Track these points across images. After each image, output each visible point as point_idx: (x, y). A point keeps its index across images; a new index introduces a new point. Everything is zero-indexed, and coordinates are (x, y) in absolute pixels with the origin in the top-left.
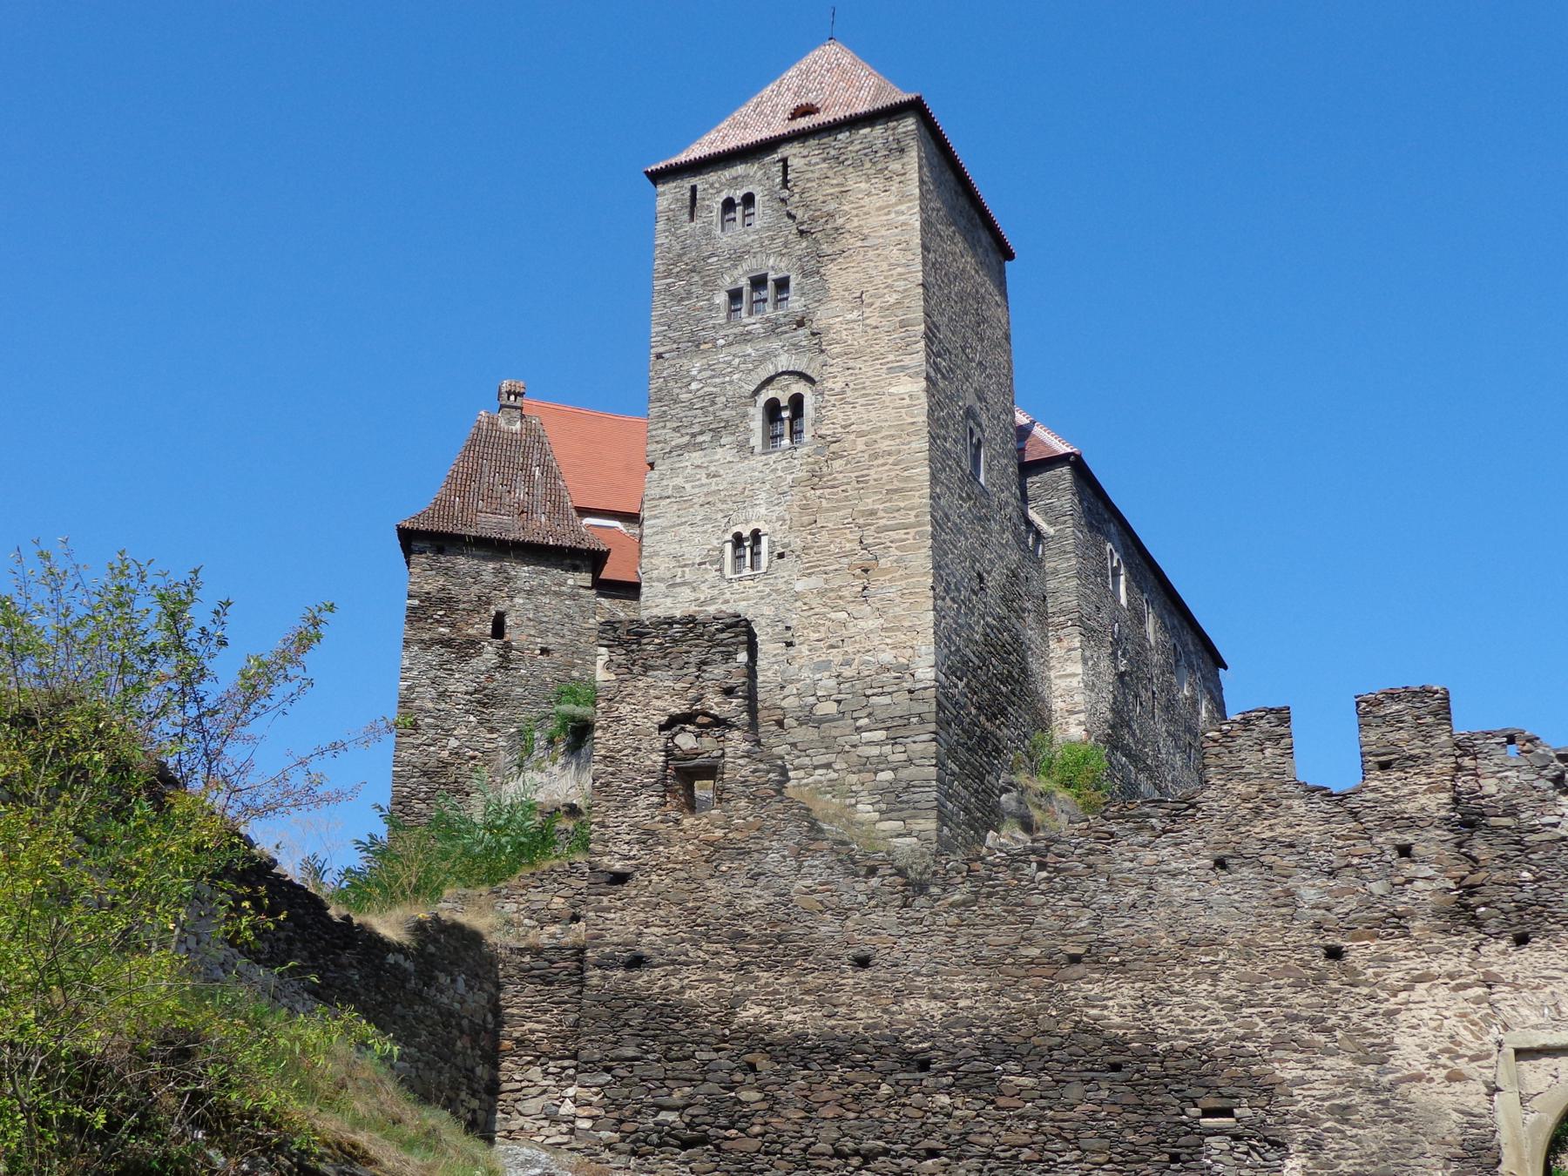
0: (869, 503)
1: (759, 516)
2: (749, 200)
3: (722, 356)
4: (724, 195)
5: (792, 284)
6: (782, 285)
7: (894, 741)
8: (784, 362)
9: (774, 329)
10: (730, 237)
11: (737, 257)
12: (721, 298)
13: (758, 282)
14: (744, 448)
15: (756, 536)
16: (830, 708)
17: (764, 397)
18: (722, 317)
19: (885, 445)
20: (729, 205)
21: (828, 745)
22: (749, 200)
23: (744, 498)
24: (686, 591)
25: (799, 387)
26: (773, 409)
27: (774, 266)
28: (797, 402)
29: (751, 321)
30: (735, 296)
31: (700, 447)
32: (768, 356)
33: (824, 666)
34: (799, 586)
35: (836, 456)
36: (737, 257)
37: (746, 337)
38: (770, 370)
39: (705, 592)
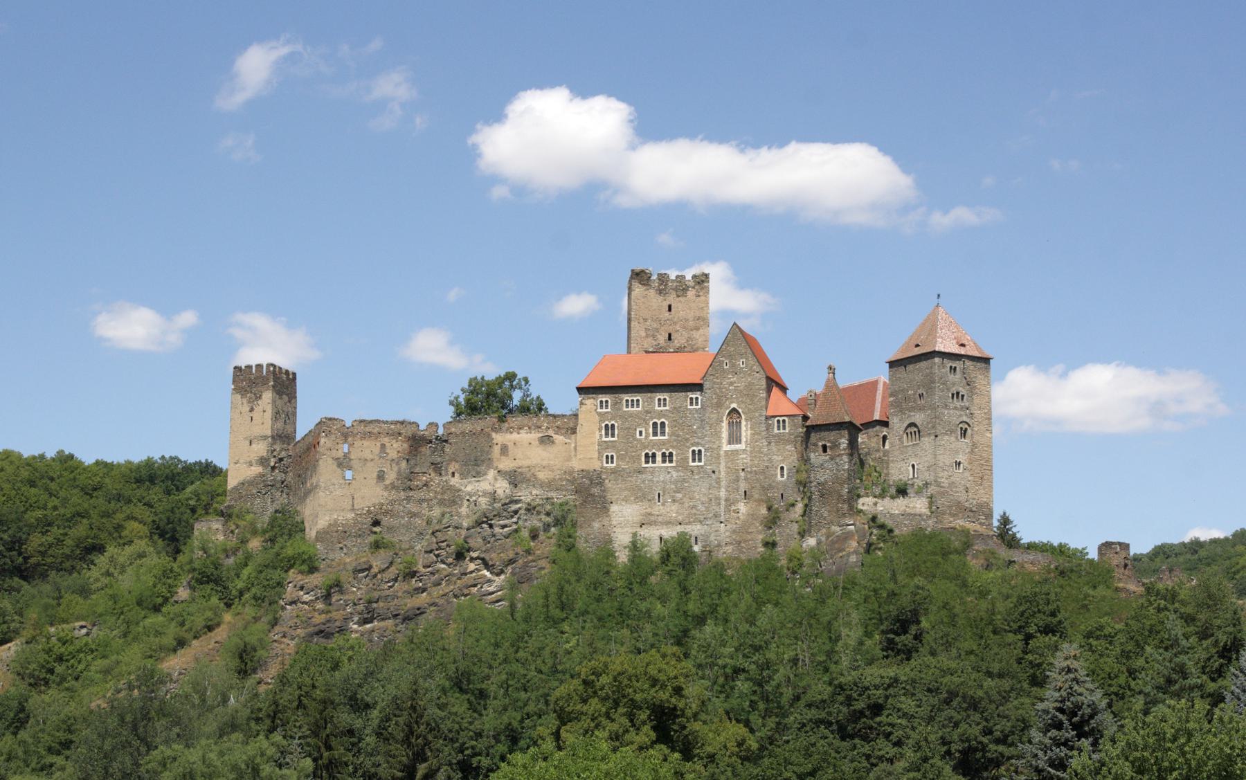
0: (982, 462)
1: (960, 458)
2: (955, 368)
3: (951, 411)
4: (950, 364)
5: (965, 397)
6: (963, 396)
7: (986, 519)
8: (965, 419)
9: (962, 408)
10: (951, 377)
11: (954, 384)
12: (950, 395)
13: (958, 393)
14: (957, 438)
15: (960, 463)
16: (974, 509)
17: (961, 425)
18: (951, 400)
19: (985, 449)
20: (951, 367)
21: (974, 517)
22: (955, 368)
23: (957, 452)
24: (946, 472)
25: (966, 426)
26: (961, 428)
27: (963, 391)
28: (966, 429)
29: (958, 404)
30: (953, 395)
31: (947, 434)
32: (961, 415)
33: (974, 499)
34: (970, 478)
35: (976, 448)
36: (954, 384)
37: (956, 408)
38: (961, 420)
39: (950, 474)
